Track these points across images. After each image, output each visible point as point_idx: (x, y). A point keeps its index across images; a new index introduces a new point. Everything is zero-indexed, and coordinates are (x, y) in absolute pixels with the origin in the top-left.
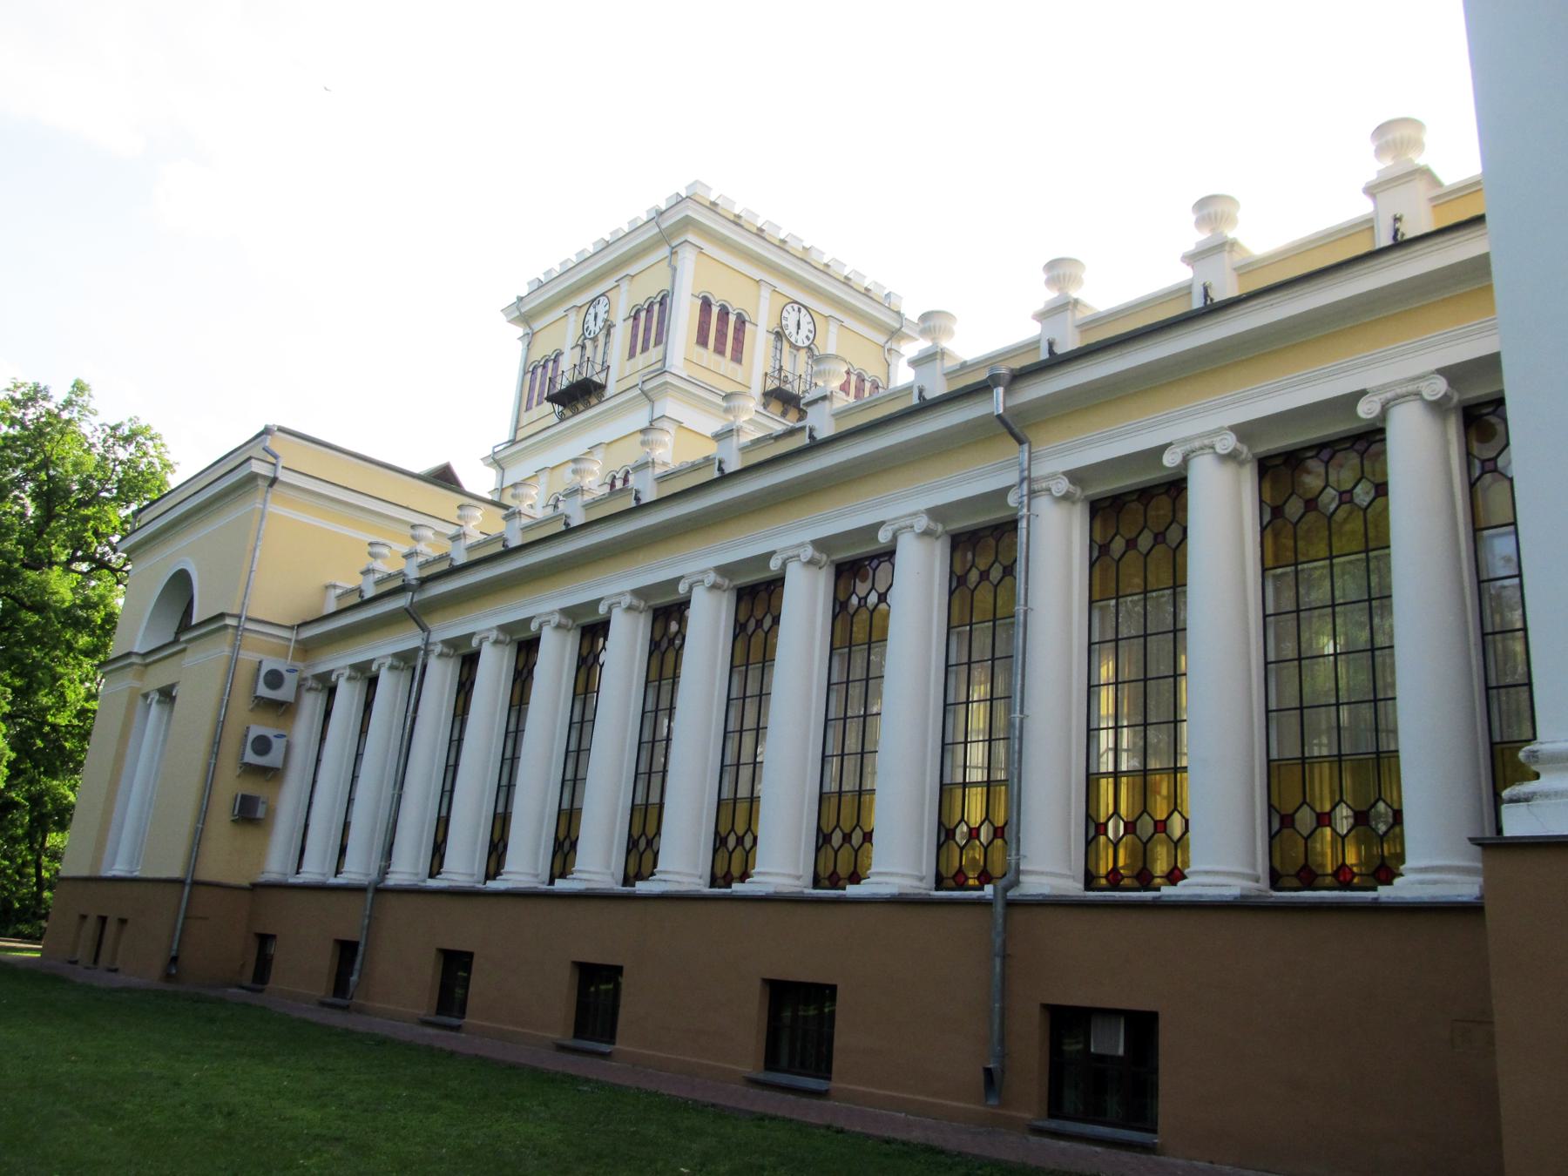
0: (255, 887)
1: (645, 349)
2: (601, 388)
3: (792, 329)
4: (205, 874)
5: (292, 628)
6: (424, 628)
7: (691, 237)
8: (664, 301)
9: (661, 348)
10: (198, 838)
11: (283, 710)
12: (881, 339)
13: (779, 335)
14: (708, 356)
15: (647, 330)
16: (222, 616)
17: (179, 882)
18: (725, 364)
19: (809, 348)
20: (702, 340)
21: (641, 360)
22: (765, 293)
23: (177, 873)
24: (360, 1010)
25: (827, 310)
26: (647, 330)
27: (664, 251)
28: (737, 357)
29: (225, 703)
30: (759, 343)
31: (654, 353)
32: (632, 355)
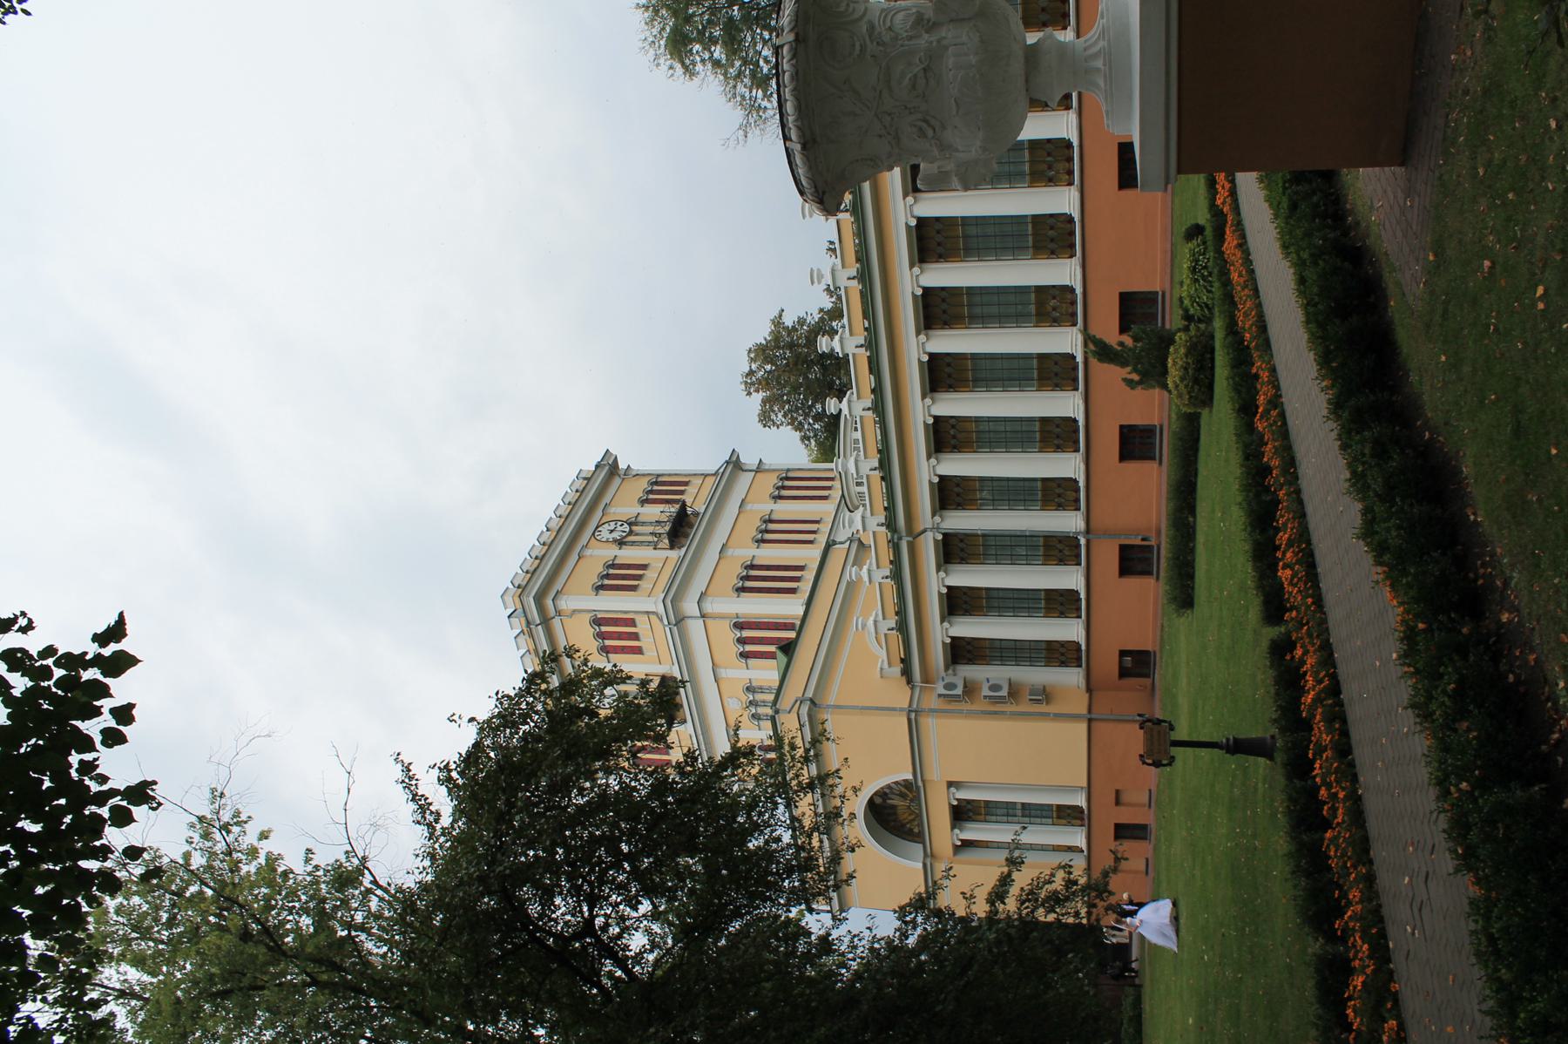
0: (1089, 689)
1: (635, 637)
2: (664, 678)
3: (616, 535)
4: (1085, 711)
5: (912, 689)
6: (925, 531)
7: (549, 603)
8: (597, 622)
9: (638, 618)
10: (1059, 717)
11: (970, 689)
12: (617, 481)
13: (621, 543)
14: (645, 585)
15: (620, 636)
16: (909, 720)
17: (1090, 721)
18: (650, 574)
19: (630, 524)
20: (633, 588)
21: (645, 642)
22: (588, 552)
23: (1083, 726)
24: (1159, 533)
25: (599, 513)
26: (620, 636)
27: (556, 623)
28: (644, 567)
29: (971, 714)
30: (629, 555)
31: (642, 627)
32: (638, 651)
